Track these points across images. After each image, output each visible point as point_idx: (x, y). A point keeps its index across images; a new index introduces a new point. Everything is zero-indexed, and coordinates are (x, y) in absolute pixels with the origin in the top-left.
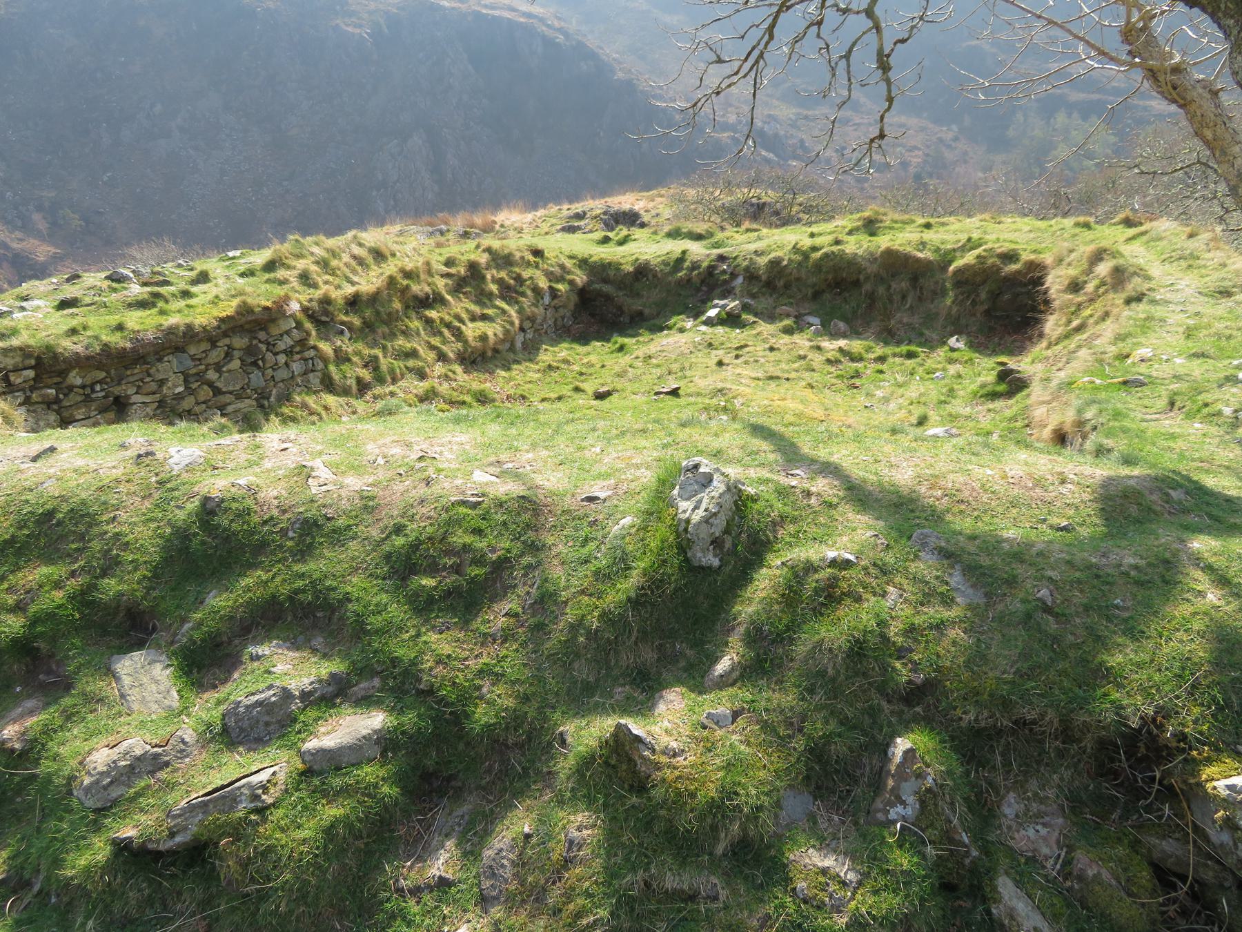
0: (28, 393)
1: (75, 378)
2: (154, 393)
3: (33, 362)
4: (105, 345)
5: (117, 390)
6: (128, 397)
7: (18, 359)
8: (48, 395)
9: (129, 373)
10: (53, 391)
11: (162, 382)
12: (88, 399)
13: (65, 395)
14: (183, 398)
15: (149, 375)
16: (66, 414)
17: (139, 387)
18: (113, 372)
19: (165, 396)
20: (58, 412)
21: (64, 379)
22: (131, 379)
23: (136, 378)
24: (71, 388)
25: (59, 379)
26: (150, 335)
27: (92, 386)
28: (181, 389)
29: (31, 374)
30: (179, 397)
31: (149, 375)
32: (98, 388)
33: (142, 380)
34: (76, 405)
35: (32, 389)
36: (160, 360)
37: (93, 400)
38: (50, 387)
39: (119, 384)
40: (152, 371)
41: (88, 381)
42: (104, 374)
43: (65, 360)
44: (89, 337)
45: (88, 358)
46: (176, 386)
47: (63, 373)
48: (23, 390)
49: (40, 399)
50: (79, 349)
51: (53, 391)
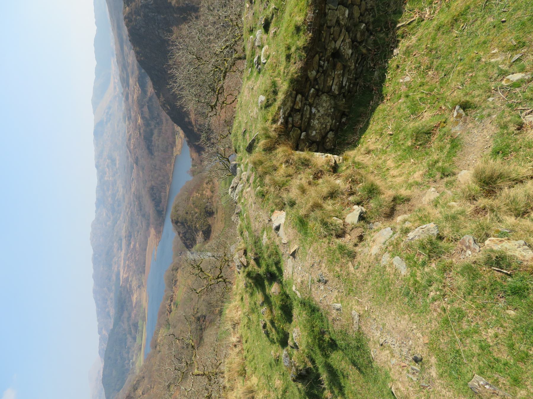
0: (307, 102)
1: (312, 74)
2: (341, 31)
3: (294, 92)
4: (304, 48)
5: (329, 53)
6: (335, 48)
7: (290, 99)
8: (313, 93)
9: (323, 40)
10: (313, 90)
11: (338, 22)
12: (325, 72)
13: (317, 84)
14: (352, 13)
15: (329, 27)
16: (326, 89)
17: (333, 39)
18: (318, 50)
19: (345, 25)
20: (323, 93)
21: (310, 80)
22: (327, 41)
23: (328, 38)
24: (315, 79)
25: (309, 83)
26: (311, 15)
27: (320, 66)
28: (347, 12)
29: (299, 97)
30: (351, 15)
31: (329, 27)
32: (322, 63)
33: (331, 34)
34: (325, 81)
35: (306, 99)
36: (325, 14)
37: (327, 70)
38: (310, 90)
39: (326, 50)
40: (329, 24)
41: (316, 66)
42: (317, 55)
43: (301, 77)
44: (295, 52)
45: (306, 63)
46: (344, 14)
47: (307, 78)
48: (305, 104)
49: (313, 99)
50: (299, 65)
51: (313, 90)
